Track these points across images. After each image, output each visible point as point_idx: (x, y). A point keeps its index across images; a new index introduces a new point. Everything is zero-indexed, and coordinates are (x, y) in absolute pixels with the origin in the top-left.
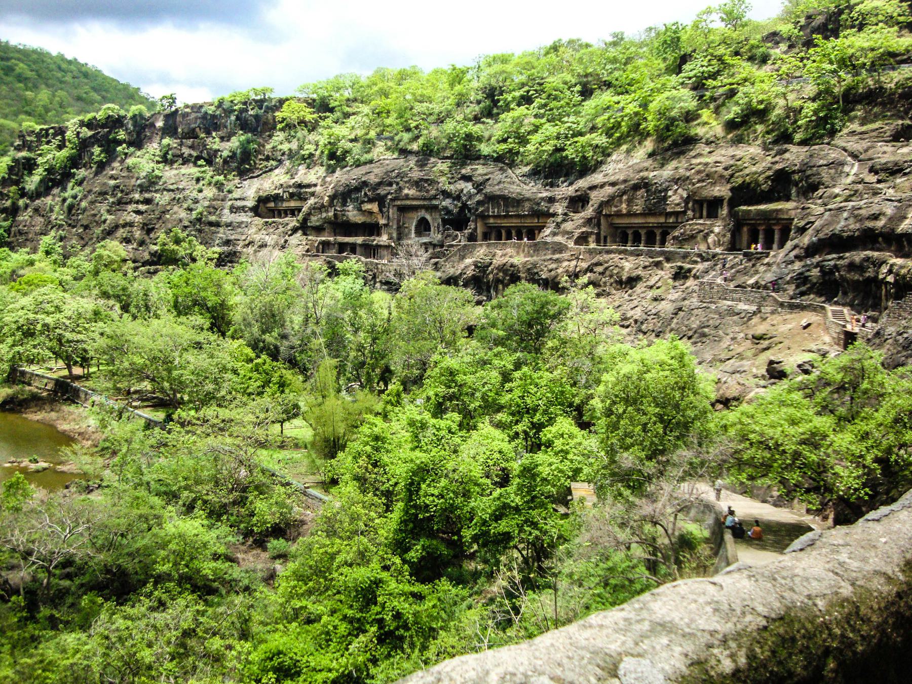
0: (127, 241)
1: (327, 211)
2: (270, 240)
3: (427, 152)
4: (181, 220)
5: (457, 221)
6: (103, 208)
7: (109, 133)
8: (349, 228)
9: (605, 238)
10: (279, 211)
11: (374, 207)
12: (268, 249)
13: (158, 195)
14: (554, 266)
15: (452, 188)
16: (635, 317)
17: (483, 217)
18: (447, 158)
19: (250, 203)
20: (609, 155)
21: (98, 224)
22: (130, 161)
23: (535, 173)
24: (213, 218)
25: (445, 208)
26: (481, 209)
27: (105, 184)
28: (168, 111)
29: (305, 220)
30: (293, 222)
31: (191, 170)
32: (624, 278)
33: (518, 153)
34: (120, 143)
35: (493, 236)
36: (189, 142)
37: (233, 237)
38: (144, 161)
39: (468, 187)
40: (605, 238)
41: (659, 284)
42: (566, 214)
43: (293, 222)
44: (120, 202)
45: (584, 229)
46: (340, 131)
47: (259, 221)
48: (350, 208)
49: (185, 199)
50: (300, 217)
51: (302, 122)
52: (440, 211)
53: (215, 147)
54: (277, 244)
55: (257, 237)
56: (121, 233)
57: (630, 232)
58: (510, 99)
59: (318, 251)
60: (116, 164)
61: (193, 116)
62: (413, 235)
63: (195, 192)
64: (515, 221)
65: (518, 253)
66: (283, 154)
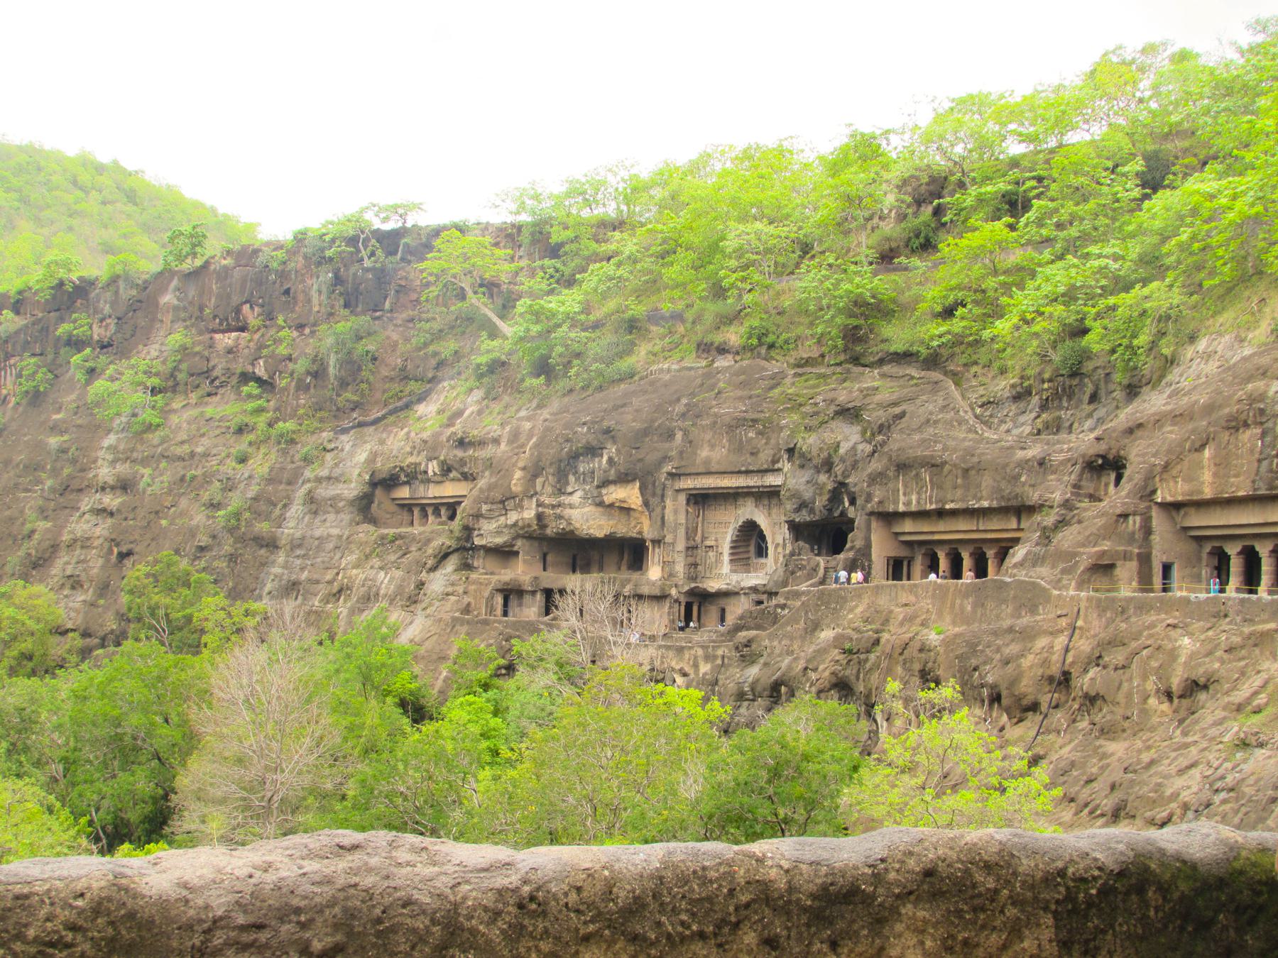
0: (75, 583)
1: (519, 507)
2: (386, 581)
3: (763, 344)
4: (193, 533)
5: (826, 533)
6: (30, 503)
7: (62, 320)
8: (579, 552)
9: (1167, 569)
10: (423, 508)
11: (630, 494)
12: (384, 604)
13: (147, 471)
14: (1013, 649)
15: (810, 442)
16: (1185, 796)
17: (889, 518)
18: (808, 362)
19: (352, 489)
20: (1192, 339)
21: (16, 540)
22: (100, 386)
23: (1021, 395)
24: (263, 527)
25: (795, 495)
26: (878, 494)
27: (40, 446)
28: (187, 266)
29: (468, 530)
30: (439, 533)
31: (227, 408)
32: (1176, 683)
33: (978, 343)
34: (77, 344)
35: (918, 567)
36: (227, 340)
37: (305, 575)
38: (121, 388)
39: (848, 437)
40: (1167, 569)
41: (1261, 699)
42: (1067, 505)
43: (439, 533)
44: (65, 489)
45: (1106, 546)
46: (567, 302)
47: (367, 533)
48: (576, 498)
49: (207, 479)
50: (456, 524)
51: (490, 287)
52: (780, 503)
53: (282, 350)
54: (400, 591)
55: (359, 575)
56: (62, 565)
57: (1233, 550)
58: (969, 201)
59: (491, 610)
60: (70, 399)
61: (237, 274)
62: (726, 568)
63: (231, 463)
64: (963, 525)
65: (940, 614)
66: (441, 365)
